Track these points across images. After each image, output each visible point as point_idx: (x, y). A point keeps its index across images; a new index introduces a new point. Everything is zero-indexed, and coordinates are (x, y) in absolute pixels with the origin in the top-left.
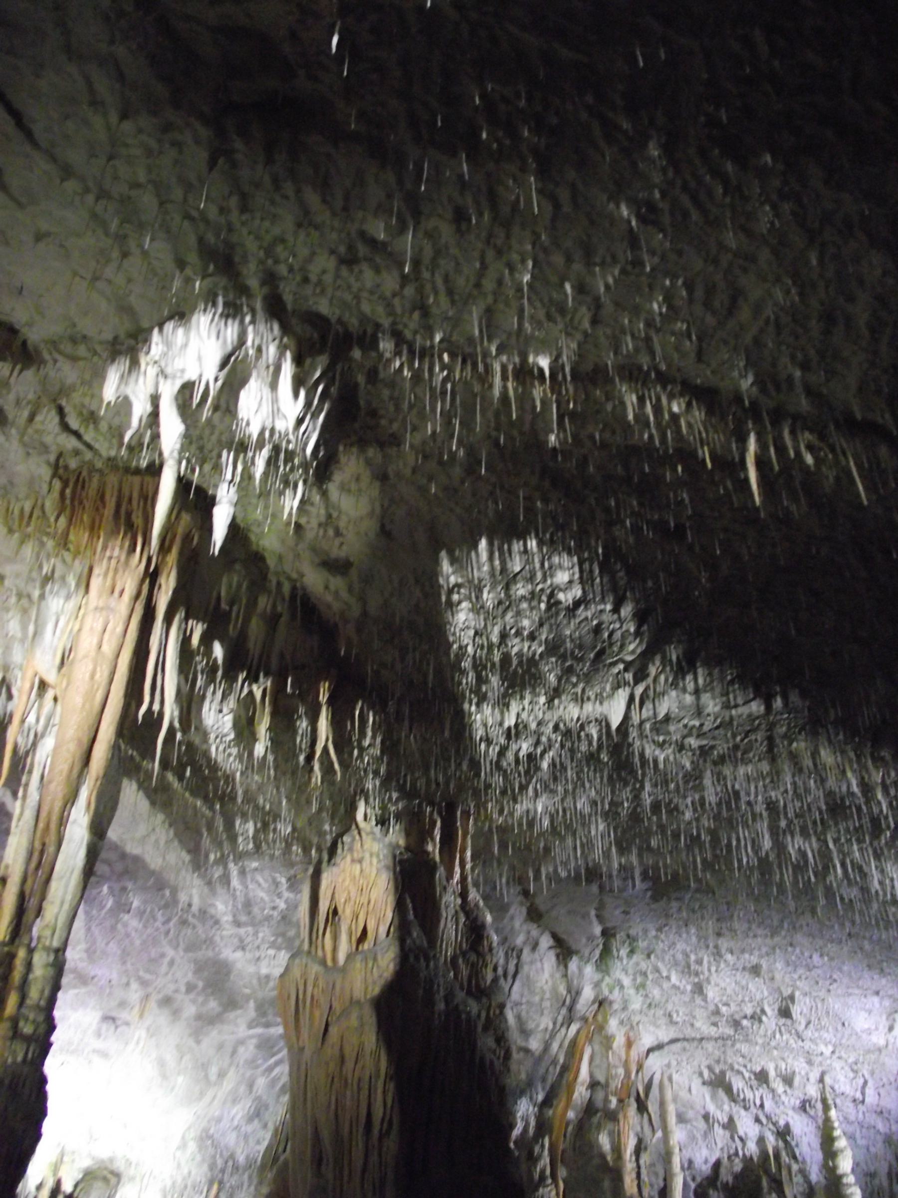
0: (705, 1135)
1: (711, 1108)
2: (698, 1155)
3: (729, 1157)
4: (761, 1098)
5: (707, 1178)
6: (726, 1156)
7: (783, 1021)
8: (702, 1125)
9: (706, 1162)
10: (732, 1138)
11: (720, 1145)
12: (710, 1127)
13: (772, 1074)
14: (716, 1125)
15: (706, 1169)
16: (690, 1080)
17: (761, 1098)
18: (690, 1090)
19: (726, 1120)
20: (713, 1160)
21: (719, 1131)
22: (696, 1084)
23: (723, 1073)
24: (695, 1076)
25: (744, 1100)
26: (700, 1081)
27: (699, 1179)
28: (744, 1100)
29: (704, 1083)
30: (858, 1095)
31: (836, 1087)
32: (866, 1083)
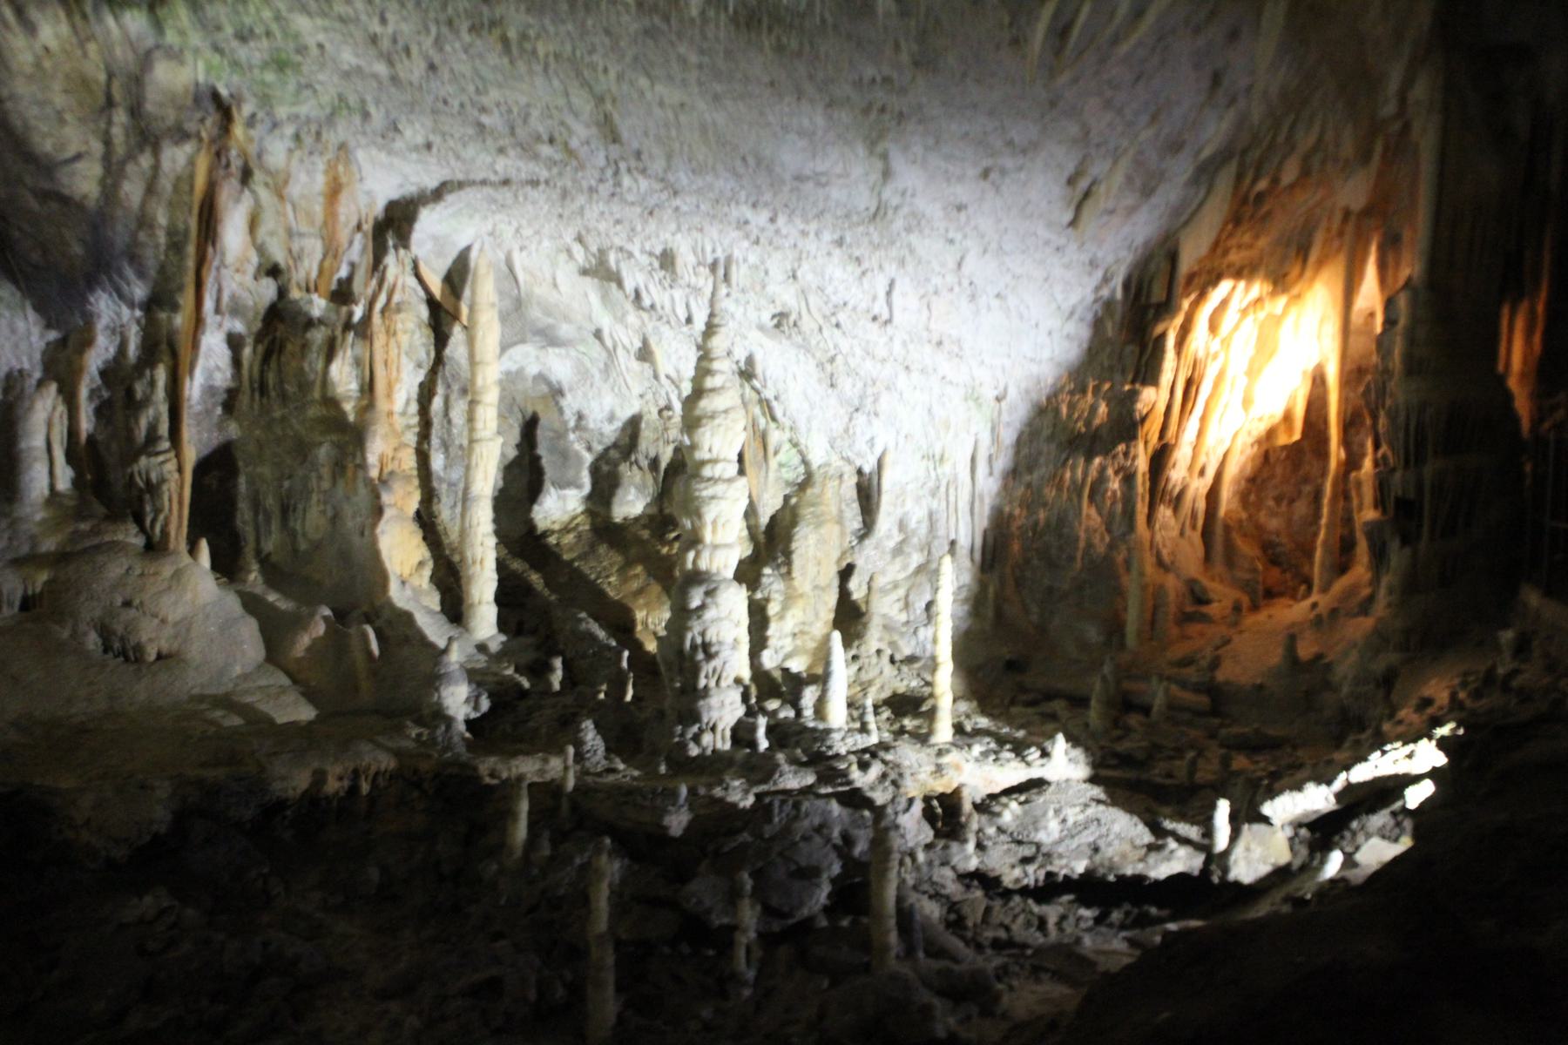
0: (606, 370)
1: (605, 321)
2: (594, 405)
3: (660, 412)
4: (687, 306)
5: (615, 445)
6: (655, 411)
7: (615, 150)
8: (595, 349)
9: (611, 418)
10: (656, 377)
11: (636, 390)
12: (611, 354)
13: (685, 258)
14: (620, 351)
15: (611, 431)
16: (554, 264)
17: (687, 306)
18: (555, 285)
19: (638, 344)
20: (625, 414)
21: (627, 362)
22: (566, 274)
23: (602, 252)
24: (563, 257)
25: (653, 306)
26: (572, 268)
27: (599, 448)
28: (653, 306)
29: (584, 272)
30: (880, 308)
31: (829, 290)
32: (892, 284)
